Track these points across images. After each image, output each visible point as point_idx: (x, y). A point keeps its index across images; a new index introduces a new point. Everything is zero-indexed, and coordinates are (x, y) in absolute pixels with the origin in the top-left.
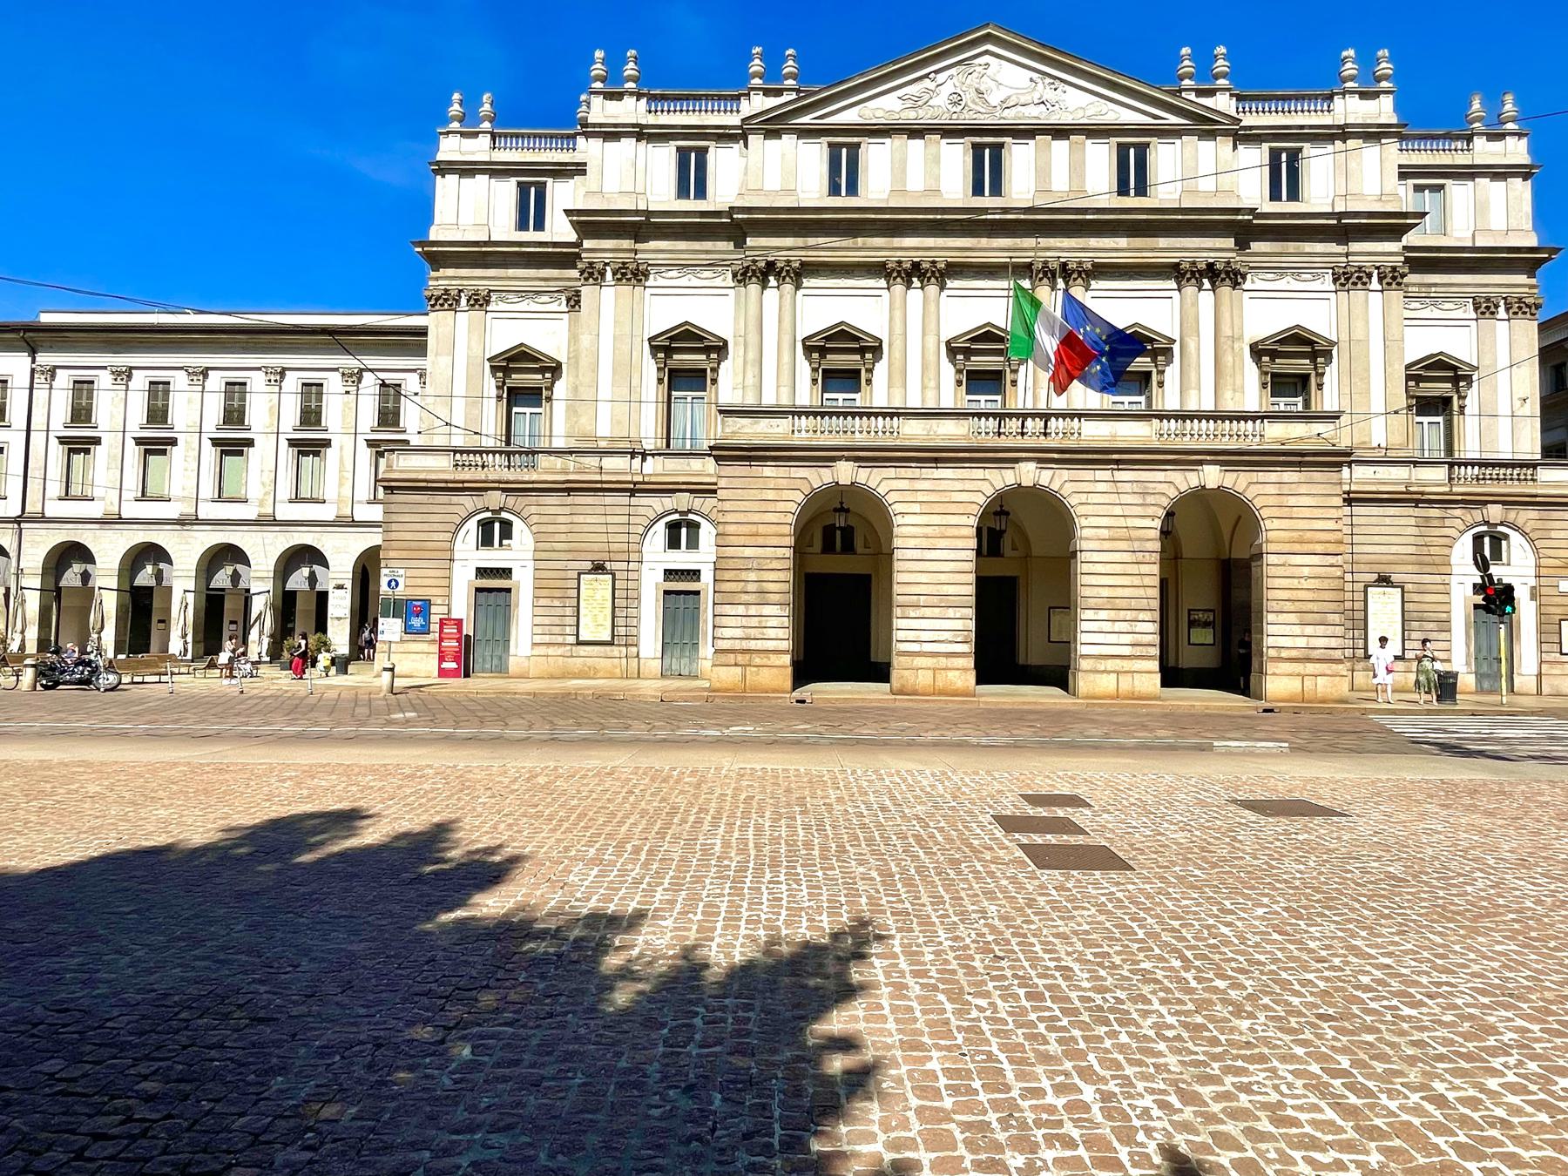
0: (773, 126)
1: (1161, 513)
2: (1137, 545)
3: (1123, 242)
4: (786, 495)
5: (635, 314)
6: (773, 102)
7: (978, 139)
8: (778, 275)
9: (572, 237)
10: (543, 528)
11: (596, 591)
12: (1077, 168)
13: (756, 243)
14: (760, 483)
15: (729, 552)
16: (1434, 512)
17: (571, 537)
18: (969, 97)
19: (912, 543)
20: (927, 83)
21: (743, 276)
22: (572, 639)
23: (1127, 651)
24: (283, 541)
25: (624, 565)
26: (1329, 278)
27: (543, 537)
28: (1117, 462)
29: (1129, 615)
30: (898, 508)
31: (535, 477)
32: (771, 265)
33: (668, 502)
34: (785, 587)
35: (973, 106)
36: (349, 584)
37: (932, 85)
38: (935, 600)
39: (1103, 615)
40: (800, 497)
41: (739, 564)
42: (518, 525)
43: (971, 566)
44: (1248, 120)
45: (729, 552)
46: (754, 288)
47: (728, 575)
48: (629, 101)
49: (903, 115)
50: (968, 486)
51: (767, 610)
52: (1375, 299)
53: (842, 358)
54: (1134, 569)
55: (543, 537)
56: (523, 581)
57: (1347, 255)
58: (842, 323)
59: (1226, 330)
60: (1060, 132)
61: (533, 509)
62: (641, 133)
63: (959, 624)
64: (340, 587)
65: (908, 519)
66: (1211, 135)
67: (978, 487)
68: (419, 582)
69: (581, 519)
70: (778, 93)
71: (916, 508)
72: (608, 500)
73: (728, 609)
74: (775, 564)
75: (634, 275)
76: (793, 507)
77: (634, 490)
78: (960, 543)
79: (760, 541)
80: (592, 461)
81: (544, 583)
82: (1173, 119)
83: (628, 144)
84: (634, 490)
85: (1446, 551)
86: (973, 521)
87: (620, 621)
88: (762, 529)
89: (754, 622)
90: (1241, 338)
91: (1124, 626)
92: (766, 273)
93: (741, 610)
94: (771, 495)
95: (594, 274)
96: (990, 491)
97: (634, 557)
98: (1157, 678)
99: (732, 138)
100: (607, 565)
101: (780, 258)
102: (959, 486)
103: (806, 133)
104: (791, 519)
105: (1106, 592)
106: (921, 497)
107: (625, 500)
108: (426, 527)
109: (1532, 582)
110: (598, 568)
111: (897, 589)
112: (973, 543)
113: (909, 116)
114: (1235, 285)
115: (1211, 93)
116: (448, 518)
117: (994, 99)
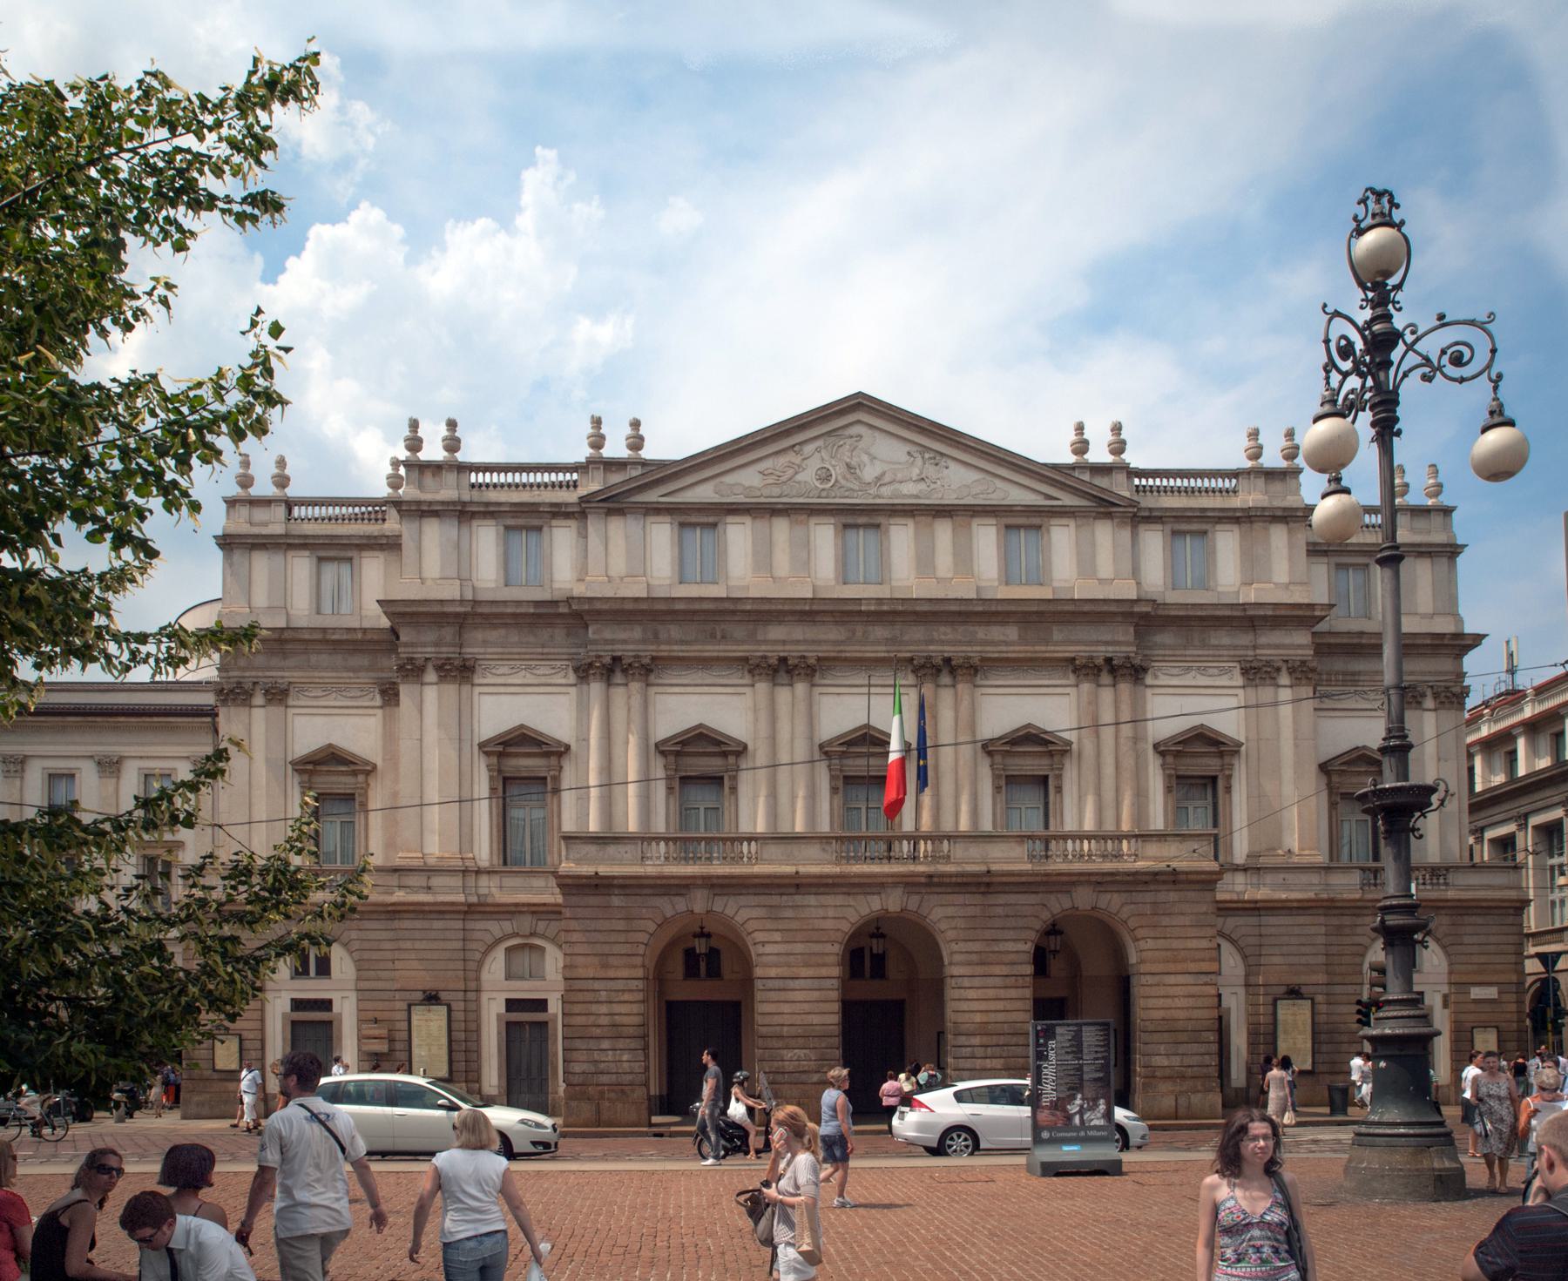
0: (612, 504)
1: (1033, 935)
2: (1005, 970)
3: (1012, 632)
4: (637, 924)
6: (616, 478)
7: (850, 520)
8: (625, 671)
9: (385, 623)
15: (578, 985)
16: (1347, 920)
18: (838, 472)
19: (773, 972)
20: (791, 457)
21: (583, 672)
26: (1237, 672)
28: (988, 885)
29: (1002, 1040)
30: (760, 936)
32: (616, 659)
34: (637, 1020)
35: (843, 482)
37: (797, 460)
38: (800, 1031)
39: (976, 1040)
40: (652, 927)
41: (589, 996)
43: (835, 995)
45: (578, 985)
46: (596, 688)
47: (577, 1009)
49: (766, 492)
50: (831, 913)
51: (621, 1044)
52: (1285, 694)
53: (700, 766)
54: (1002, 993)
57: (1255, 647)
58: (701, 726)
65: (769, 949)
71: (777, 937)
73: (578, 1044)
74: (626, 997)
78: (824, 972)
79: (611, 974)
85: (1357, 960)
89: (610, 1056)
92: (612, 669)
93: (592, 1044)
95: (413, 671)
96: (854, 917)
97: (472, 985)
99: (567, 515)
101: (627, 651)
102: (821, 912)
111: (759, 1019)
112: (836, 971)
113: (772, 495)
117: (869, 473)
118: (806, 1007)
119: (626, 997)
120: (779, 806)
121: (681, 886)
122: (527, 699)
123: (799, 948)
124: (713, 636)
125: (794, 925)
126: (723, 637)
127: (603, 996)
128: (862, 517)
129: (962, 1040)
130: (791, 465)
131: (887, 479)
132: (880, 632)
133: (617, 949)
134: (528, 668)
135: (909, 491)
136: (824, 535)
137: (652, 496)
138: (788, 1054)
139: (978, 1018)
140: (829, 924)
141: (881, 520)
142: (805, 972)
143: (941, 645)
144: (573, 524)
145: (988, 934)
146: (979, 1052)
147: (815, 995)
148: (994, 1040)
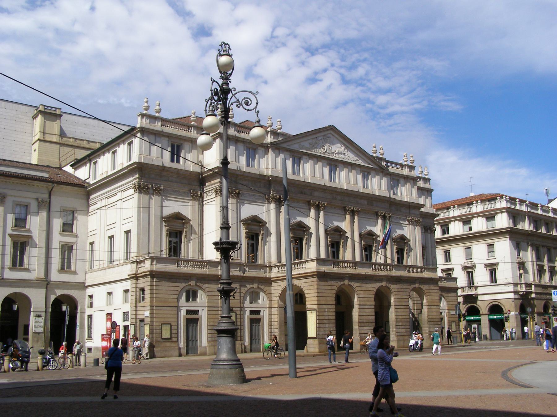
4: (334, 288)
10: (210, 293)
23: (405, 334)
25: (239, 309)
27: (210, 297)
39: (400, 324)
40: (336, 289)
42: (200, 293)
43: (373, 310)
55: (210, 297)
56: (204, 316)
61: (207, 286)
65: (361, 296)
66: (382, 172)
67: (374, 287)
68: (165, 316)
71: (362, 292)
74: (331, 310)
76: (335, 292)
81: (212, 316)
86: (373, 296)
93: (324, 325)
100: (234, 309)
105: (400, 317)
106: (363, 289)
108: (168, 292)
109: (446, 311)
112: (373, 303)
116: (176, 288)
118: (368, 314)
123: (366, 296)
124: (302, 193)
125: (365, 289)
126: (305, 194)
127: (326, 310)
130: (316, 143)
131: (337, 152)
132: (339, 197)
133: (330, 295)
134: (254, 195)
135: (341, 157)
137: (285, 145)
138: (365, 328)
140: (372, 289)
141: (337, 164)
144: (263, 149)
145: (401, 293)
147: (370, 310)
148: (404, 324)
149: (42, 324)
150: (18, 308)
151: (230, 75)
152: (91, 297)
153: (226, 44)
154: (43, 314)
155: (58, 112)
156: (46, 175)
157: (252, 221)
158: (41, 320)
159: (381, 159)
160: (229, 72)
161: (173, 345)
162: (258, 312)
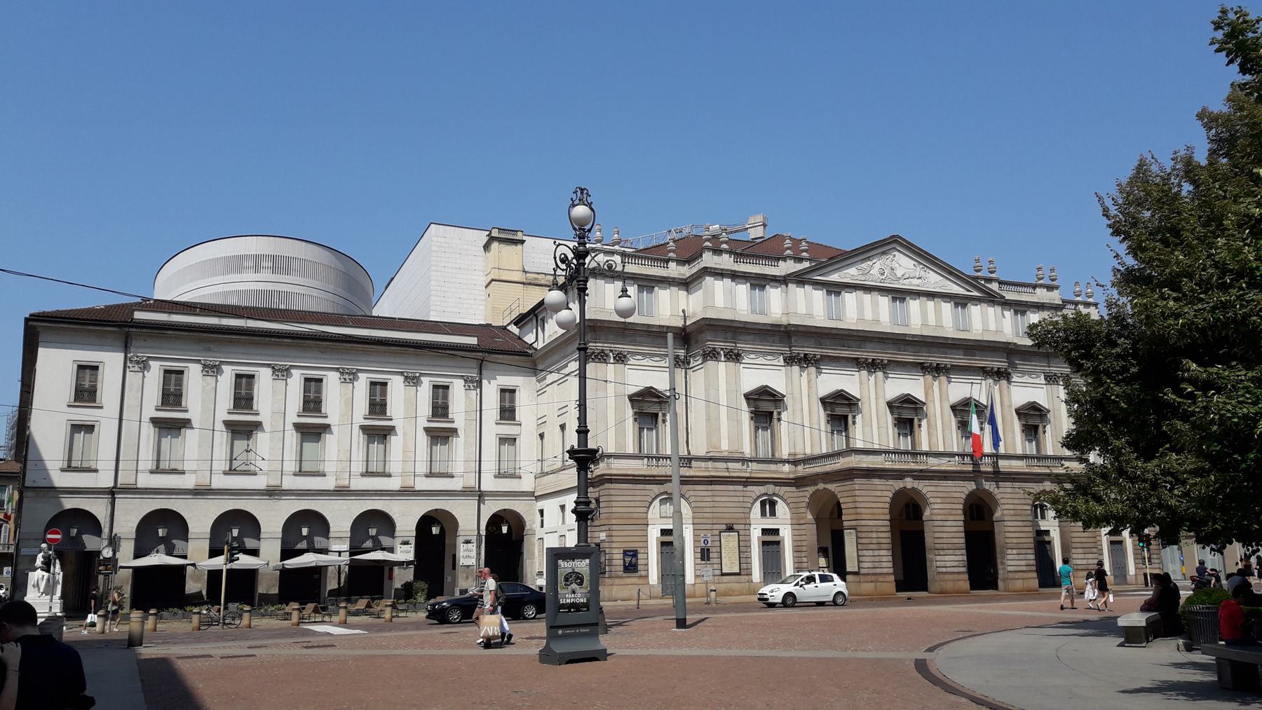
0: (799, 279)
5: (737, 376)
11: (730, 542)
12: (938, 312)
13: (801, 344)
14: (873, 487)
17: (715, 510)
19: (939, 518)
21: (790, 360)
22: (718, 572)
23: (1024, 568)
24: (422, 507)
30: (932, 500)
31: (692, 473)
33: (762, 489)
36: (413, 541)
37: (870, 263)
43: (962, 529)
44: (1010, 296)
46: (796, 368)
47: (863, 535)
48: (726, 256)
51: (882, 552)
53: (840, 410)
59: (1006, 403)
60: (931, 295)
61: (692, 493)
62: (735, 276)
63: (960, 558)
64: (406, 543)
65: (936, 506)
69: (718, 499)
70: (800, 260)
72: (731, 487)
73: (865, 553)
74: (883, 529)
75: (734, 357)
76: (888, 500)
77: (747, 482)
78: (958, 518)
80: (722, 465)
82: (975, 293)
83: (727, 281)
84: (747, 482)
86: (961, 507)
87: (743, 561)
88: (877, 511)
89: (877, 559)
90: (1010, 406)
91: (1022, 557)
92: (805, 361)
93: (871, 553)
94: (878, 493)
98: (1037, 581)
100: (735, 527)
103: (818, 284)
104: (887, 506)
107: (741, 488)
108: (632, 504)
110: (730, 529)
112: (962, 518)
114: (1009, 382)
115: (990, 280)
117: (899, 273)
119: (883, 529)
120: (873, 429)
121: (900, 474)
122: (762, 371)
128: (899, 295)
129: (1009, 551)
133: (881, 505)
136: (884, 301)
138: (947, 558)
139: (1015, 541)
142: (951, 518)
143: (934, 356)
146: (1016, 557)
149: (474, 554)
150: (442, 530)
151: (589, 230)
152: (542, 512)
153: (582, 190)
154: (474, 539)
155: (519, 236)
156: (473, 341)
157: (759, 394)
158: (473, 547)
159: (990, 280)
160: (587, 227)
161: (641, 581)
162: (776, 531)
